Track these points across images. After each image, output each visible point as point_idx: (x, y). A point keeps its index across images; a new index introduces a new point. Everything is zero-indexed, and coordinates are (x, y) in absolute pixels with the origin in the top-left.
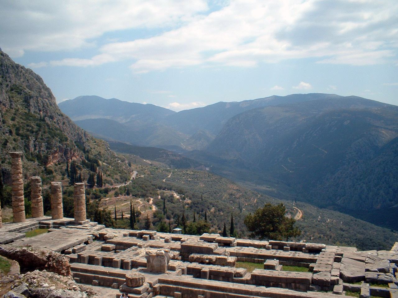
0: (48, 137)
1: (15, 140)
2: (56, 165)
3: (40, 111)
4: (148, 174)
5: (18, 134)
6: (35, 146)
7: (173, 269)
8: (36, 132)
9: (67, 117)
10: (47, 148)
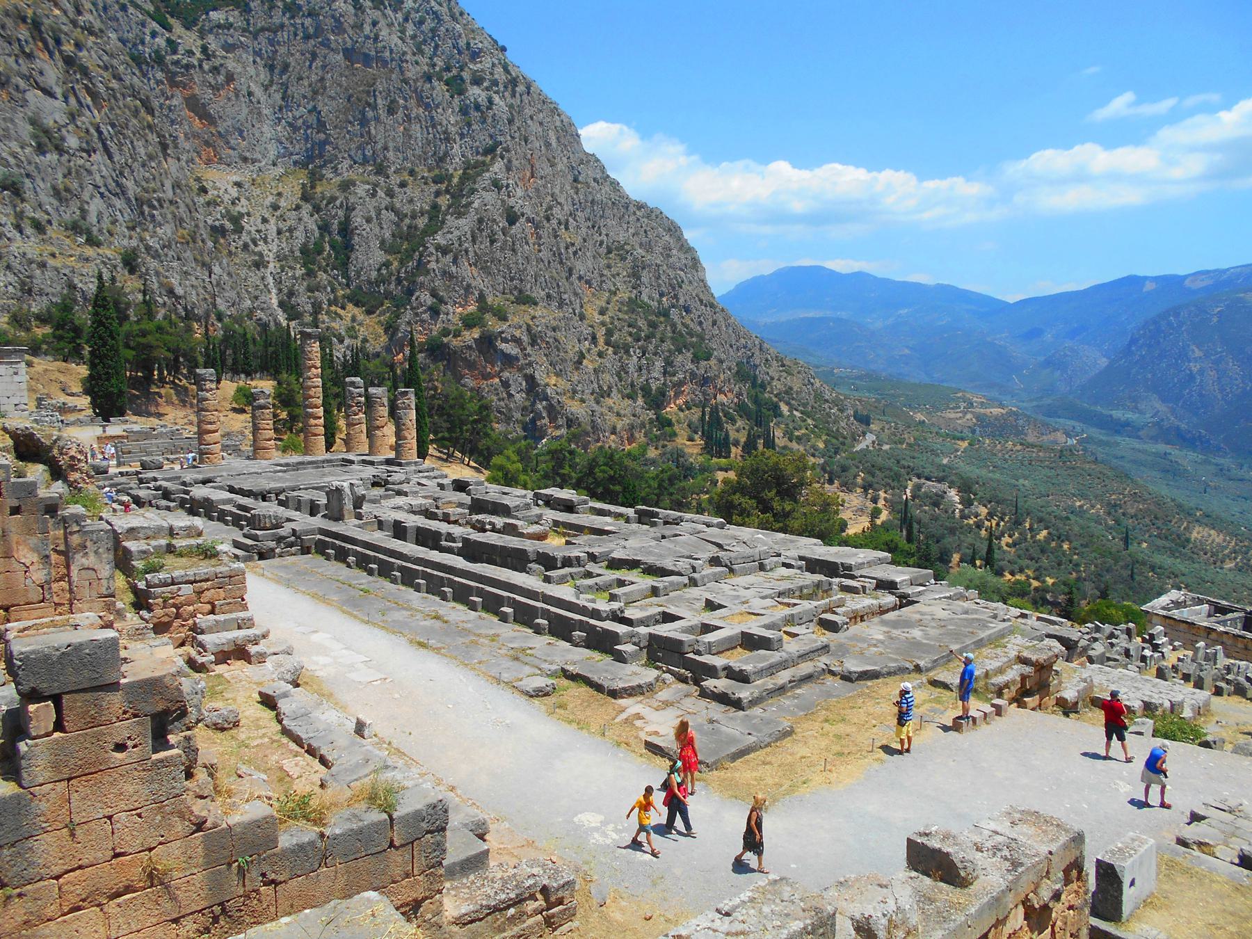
0: (669, 351)
1: (600, 355)
2: (681, 409)
3: (662, 295)
4: (909, 445)
5: (608, 343)
6: (640, 369)
7: (359, 517)
8: (648, 338)
9: (723, 310)
10: (665, 374)
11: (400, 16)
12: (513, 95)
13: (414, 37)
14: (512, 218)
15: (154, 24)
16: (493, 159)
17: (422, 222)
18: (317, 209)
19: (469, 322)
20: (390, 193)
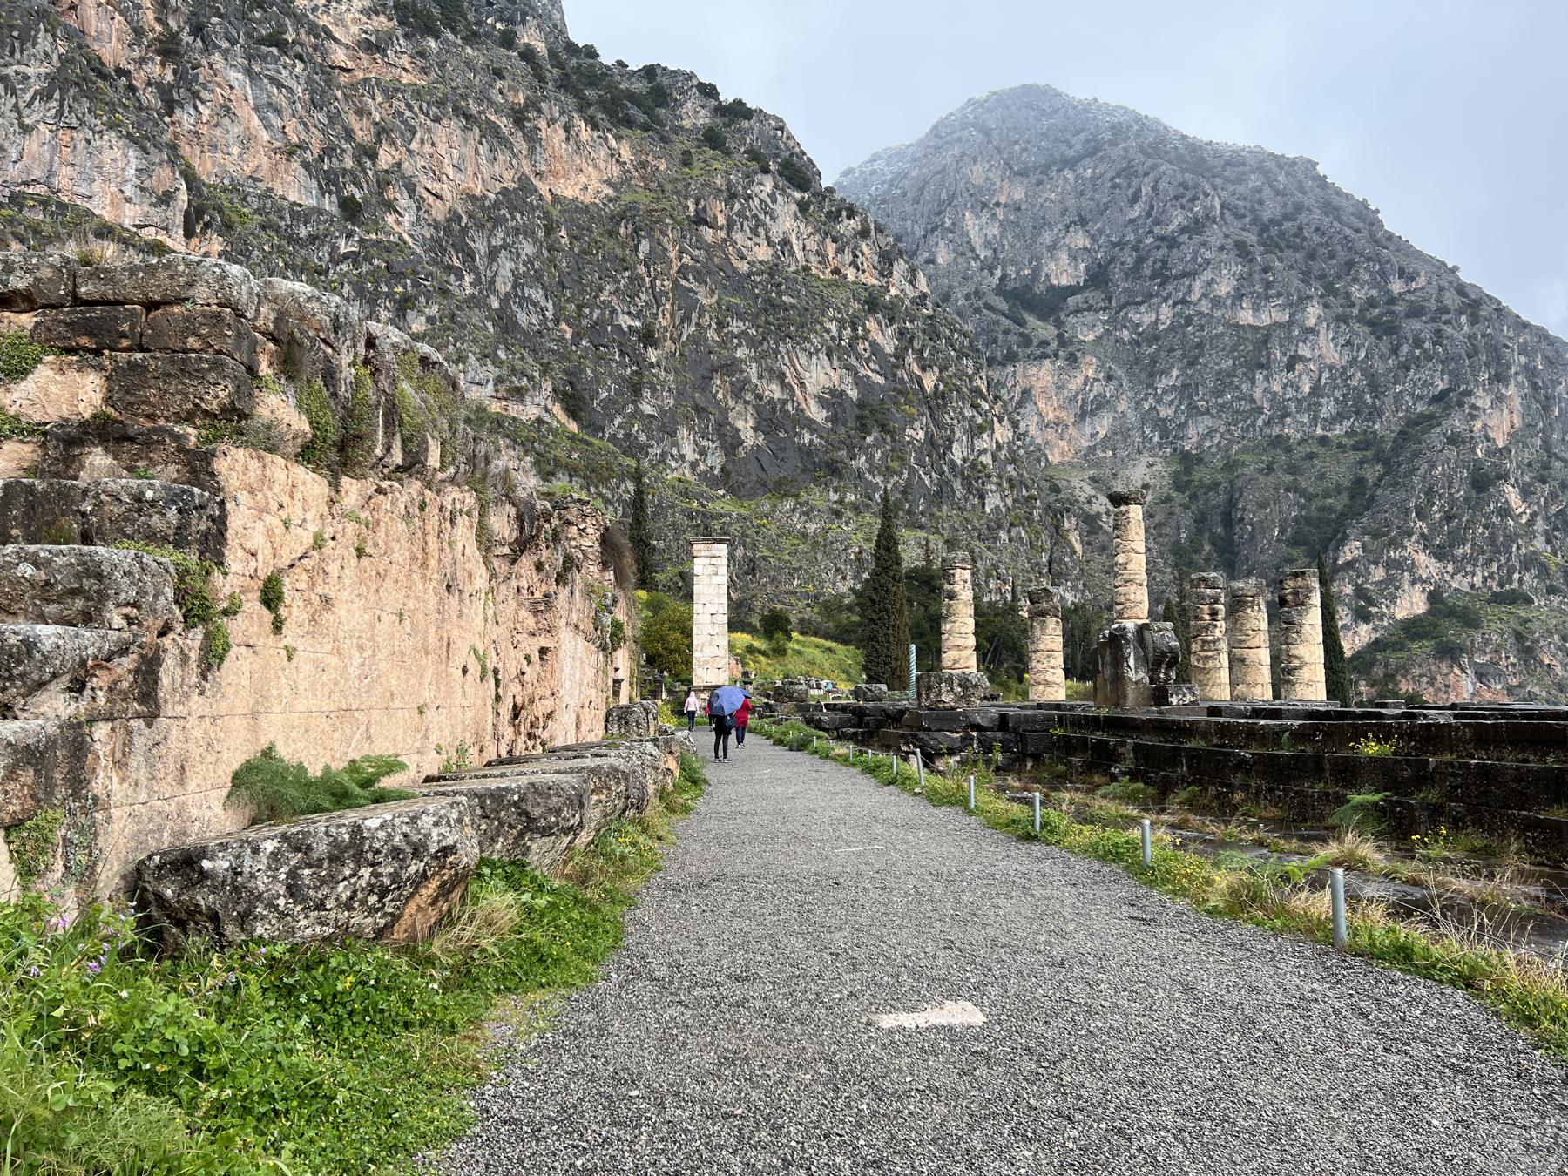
11: (1298, 256)
12: (1474, 320)
13: (1321, 277)
14: (1483, 482)
15: (1008, 322)
16: (1445, 409)
17: (1339, 503)
18: (1193, 497)
19: (1413, 629)
20: (1292, 469)
